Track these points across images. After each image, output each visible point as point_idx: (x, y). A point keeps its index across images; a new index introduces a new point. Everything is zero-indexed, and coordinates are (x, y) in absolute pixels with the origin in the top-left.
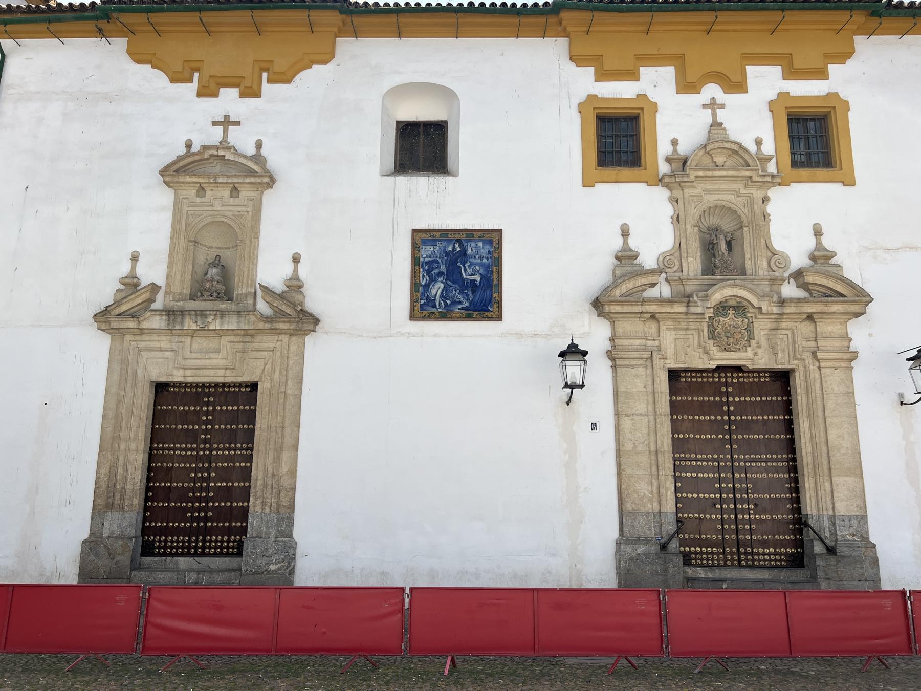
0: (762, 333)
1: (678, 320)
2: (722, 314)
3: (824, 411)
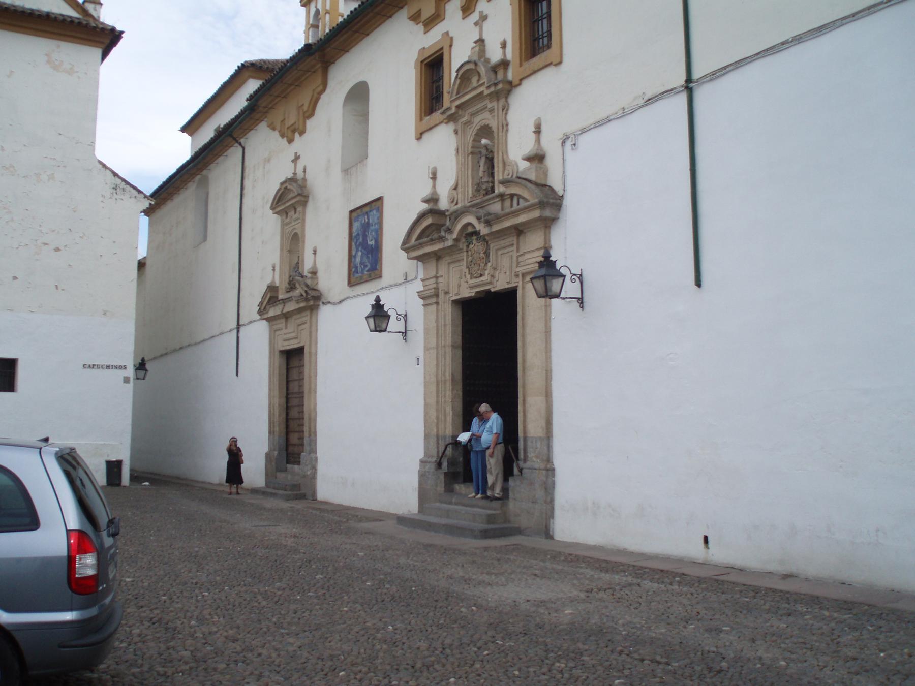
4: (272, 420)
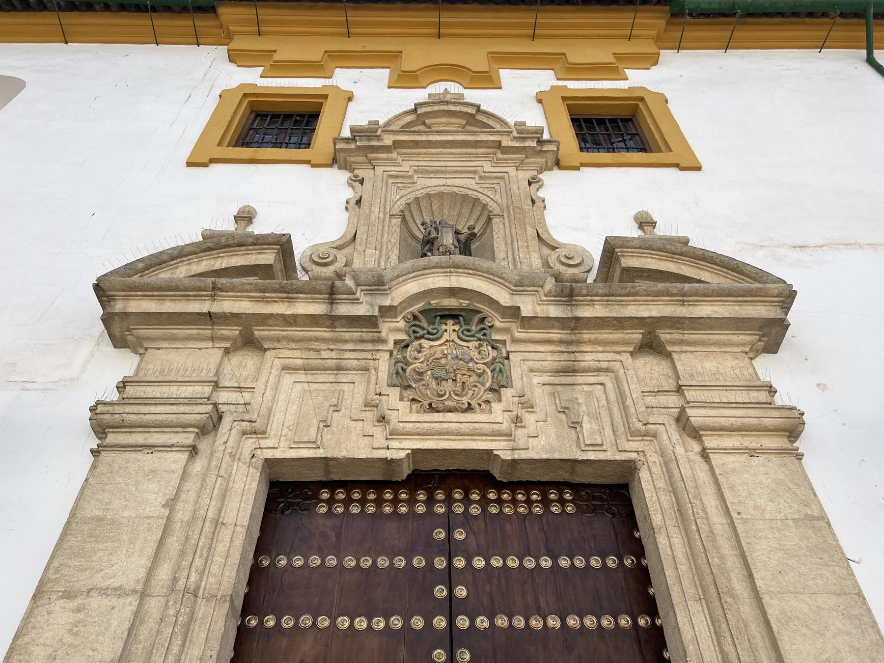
0: (536, 380)
1: (315, 345)
2: (429, 333)
3: (750, 576)
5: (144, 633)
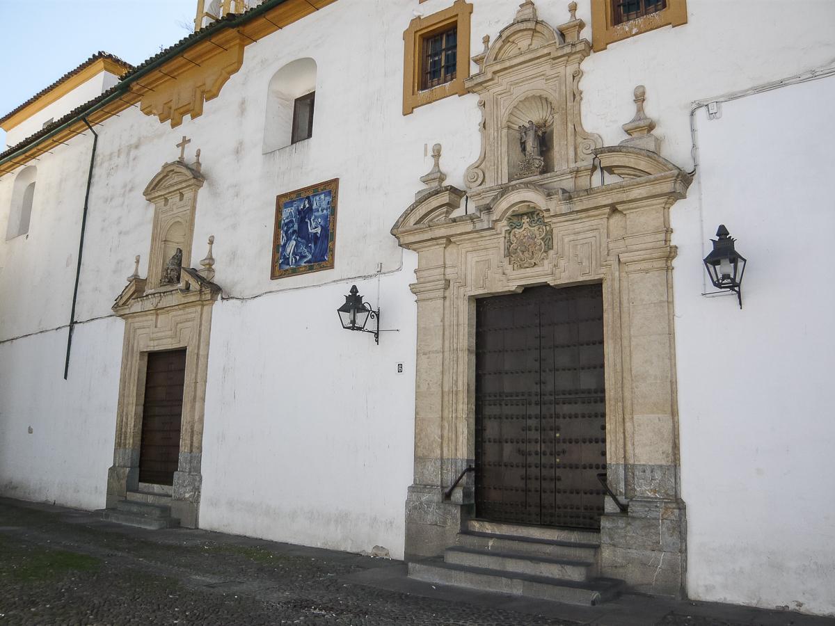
1: (475, 240)
4: (123, 430)
5: (446, 362)
